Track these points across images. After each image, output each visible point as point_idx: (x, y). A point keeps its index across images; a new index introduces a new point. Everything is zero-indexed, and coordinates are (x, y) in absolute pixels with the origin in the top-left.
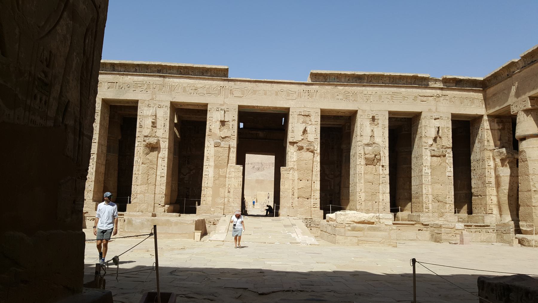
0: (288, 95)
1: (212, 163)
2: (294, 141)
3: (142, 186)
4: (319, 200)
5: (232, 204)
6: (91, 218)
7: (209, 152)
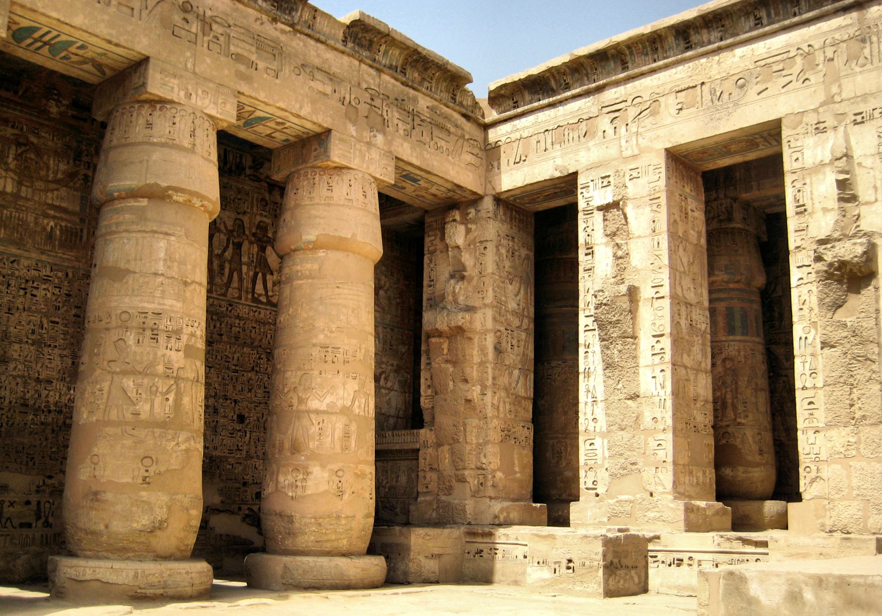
3: (833, 433)
6: (670, 558)
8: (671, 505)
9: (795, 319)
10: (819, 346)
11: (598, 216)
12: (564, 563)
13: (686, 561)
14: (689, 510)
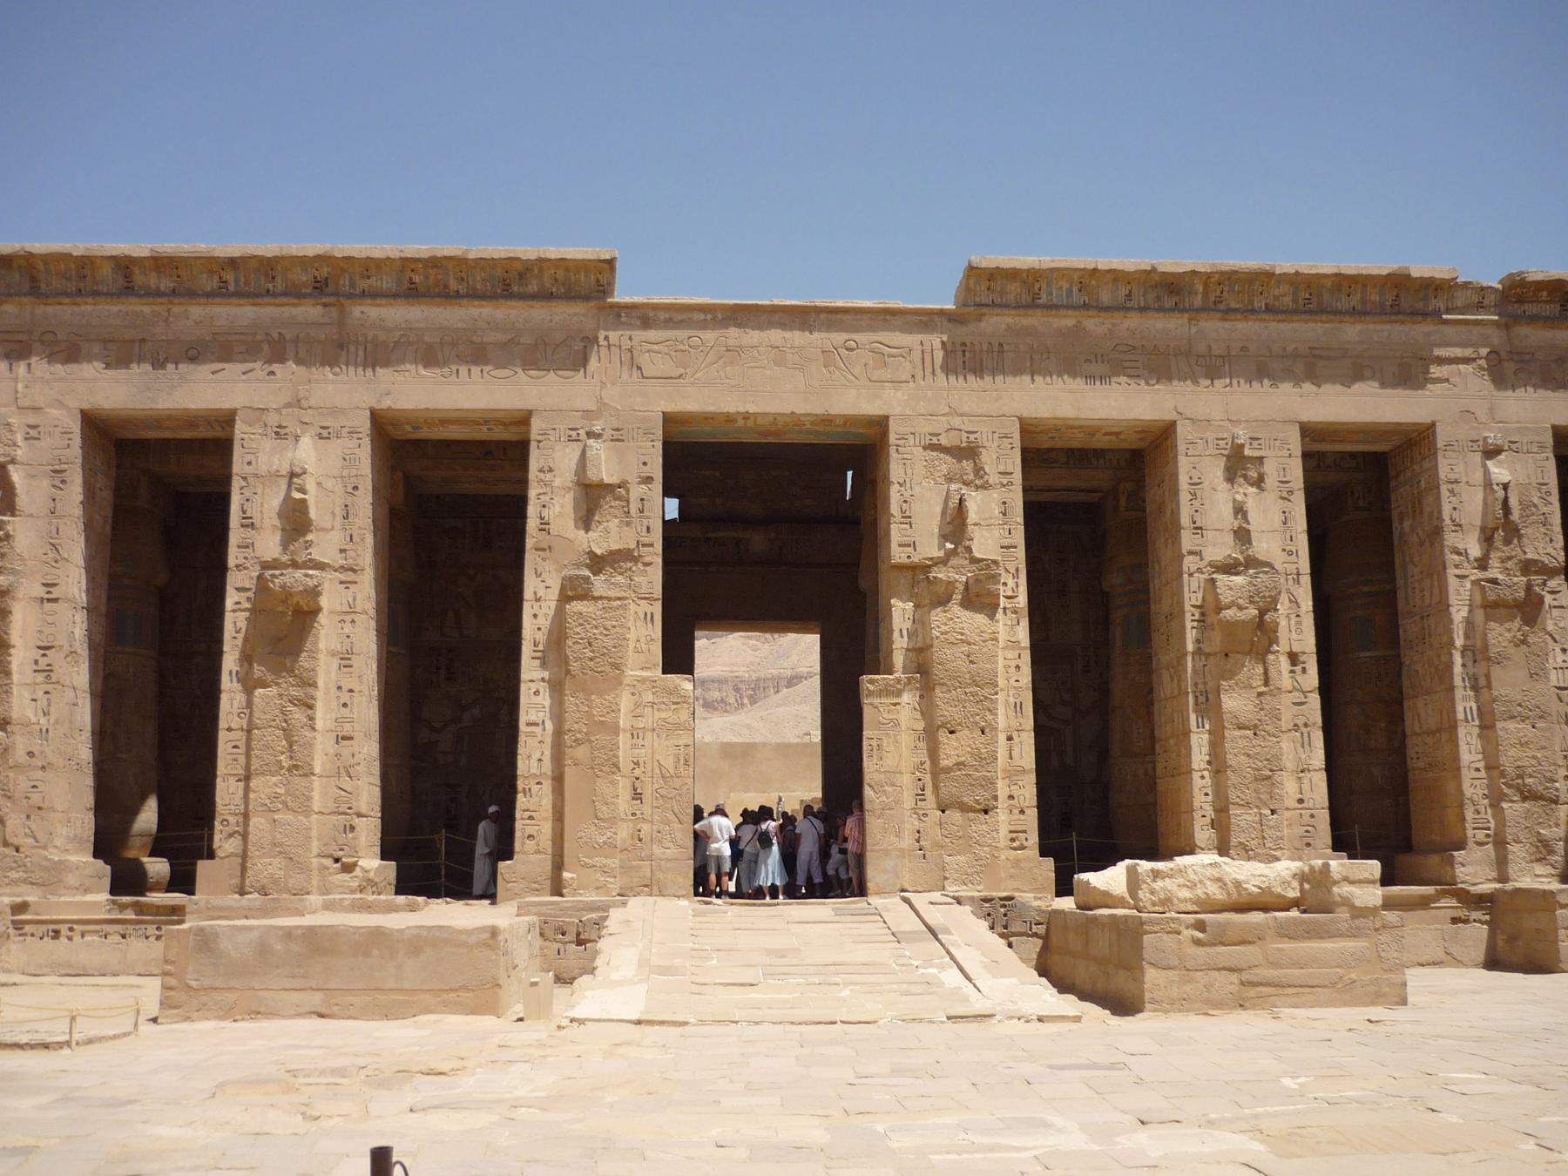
2: (916, 559)
4: (1032, 814)
5: (657, 850)
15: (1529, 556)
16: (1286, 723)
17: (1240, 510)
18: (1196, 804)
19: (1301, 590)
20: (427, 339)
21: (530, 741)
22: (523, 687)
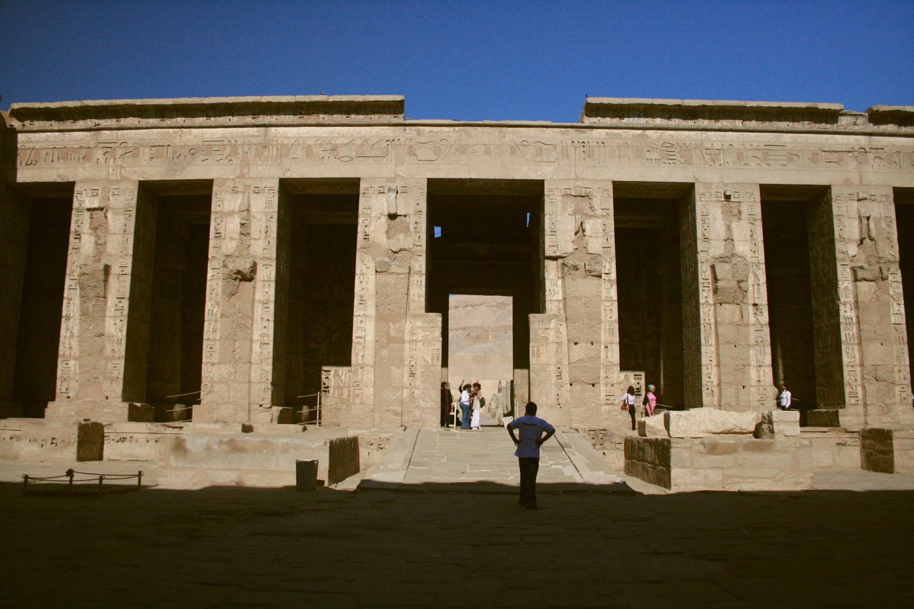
0: (539, 152)
1: (371, 311)
3: (223, 366)
5: (422, 403)
7: (364, 285)
8: (121, 405)
9: (207, 299)
10: (219, 316)
11: (87, 215)
12: (49, 441)
13: (128, 439)
14: (132, 408)
15: (881, 255)
16: (752, 342)
17: (729, 228)
18: (704, 383)
19: (760, 272)
20: (308, 142)
21: (358, 346)
22: (355, 319)
